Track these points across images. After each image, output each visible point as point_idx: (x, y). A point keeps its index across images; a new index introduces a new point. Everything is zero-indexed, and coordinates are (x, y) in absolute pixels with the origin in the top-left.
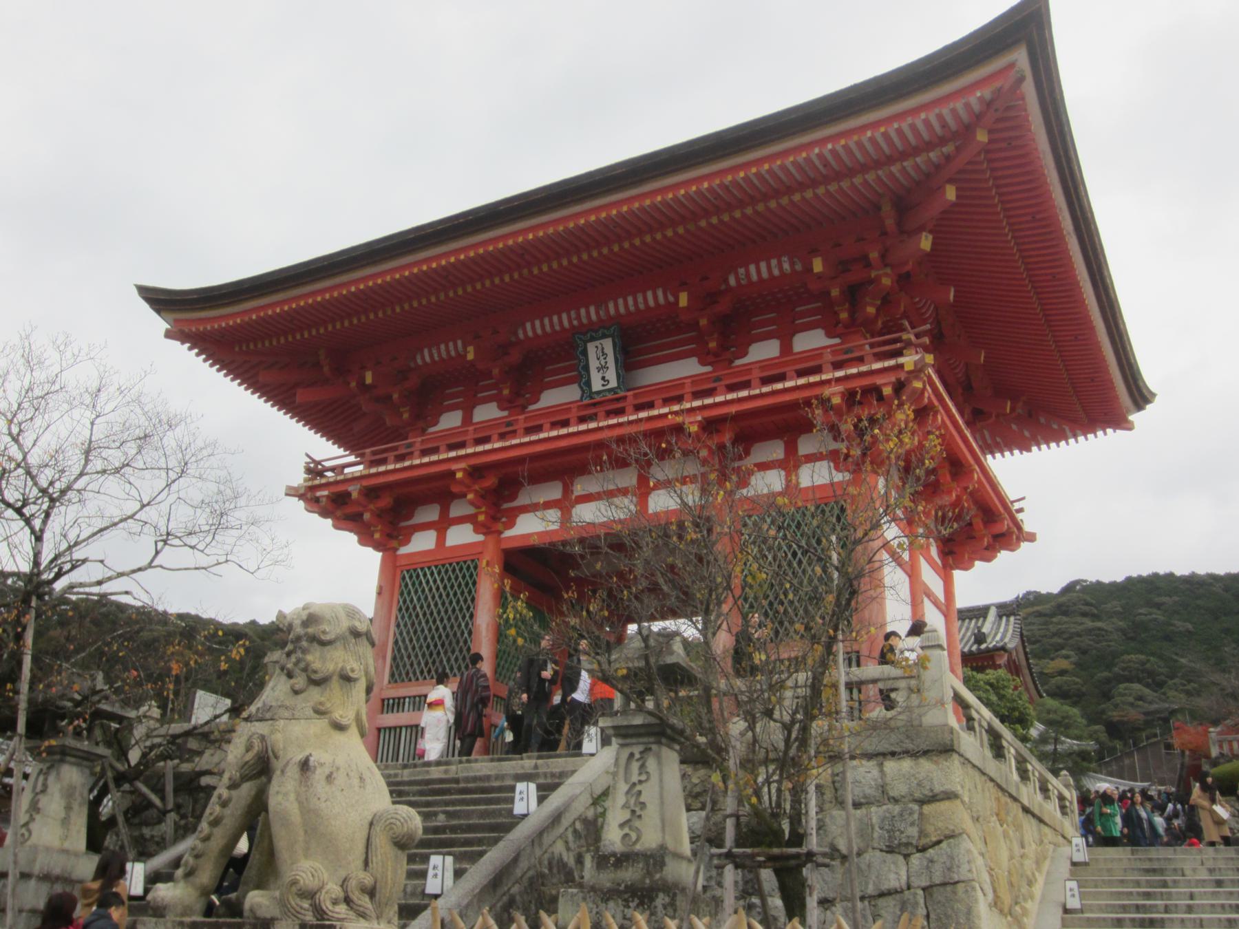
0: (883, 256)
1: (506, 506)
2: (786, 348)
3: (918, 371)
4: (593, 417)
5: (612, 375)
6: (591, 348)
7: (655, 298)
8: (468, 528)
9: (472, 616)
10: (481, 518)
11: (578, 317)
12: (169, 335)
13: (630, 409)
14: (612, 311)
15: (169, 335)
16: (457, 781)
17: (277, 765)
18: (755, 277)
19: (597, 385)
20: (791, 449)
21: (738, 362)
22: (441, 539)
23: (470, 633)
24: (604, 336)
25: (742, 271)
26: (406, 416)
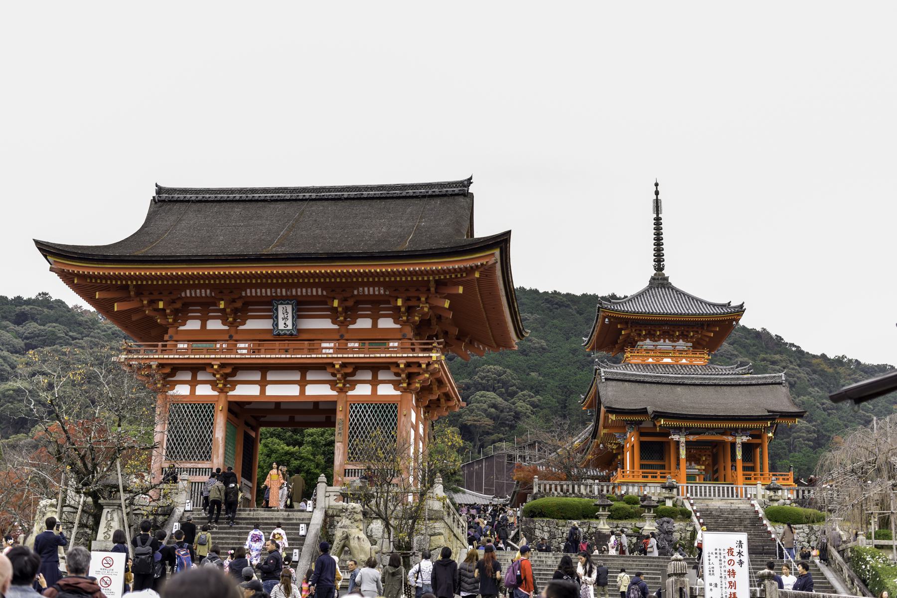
0: (426, 299)
1: (229, 379)
2: (375, 324)
3: (438, 361)
4: (287, 351)
5: (289, 323)
6: (280, 308)
7: (317, 291)
8: (209, 387)
9: (212, 432)
10: (220, 386)
11: (276, 292)
12: (51, 270)
13: (306, 351)
14: (294, 293)
15: (51, 270)
16: (258, 519)
17: (351, 537)
18: (366, 293)
19: (281, 326)
20: (375, 376)
21: (351, 327)
22: (193, 391)
23: (211, 440)
24: (288, 304)
25: (361, 289)
26: (170, 320)
